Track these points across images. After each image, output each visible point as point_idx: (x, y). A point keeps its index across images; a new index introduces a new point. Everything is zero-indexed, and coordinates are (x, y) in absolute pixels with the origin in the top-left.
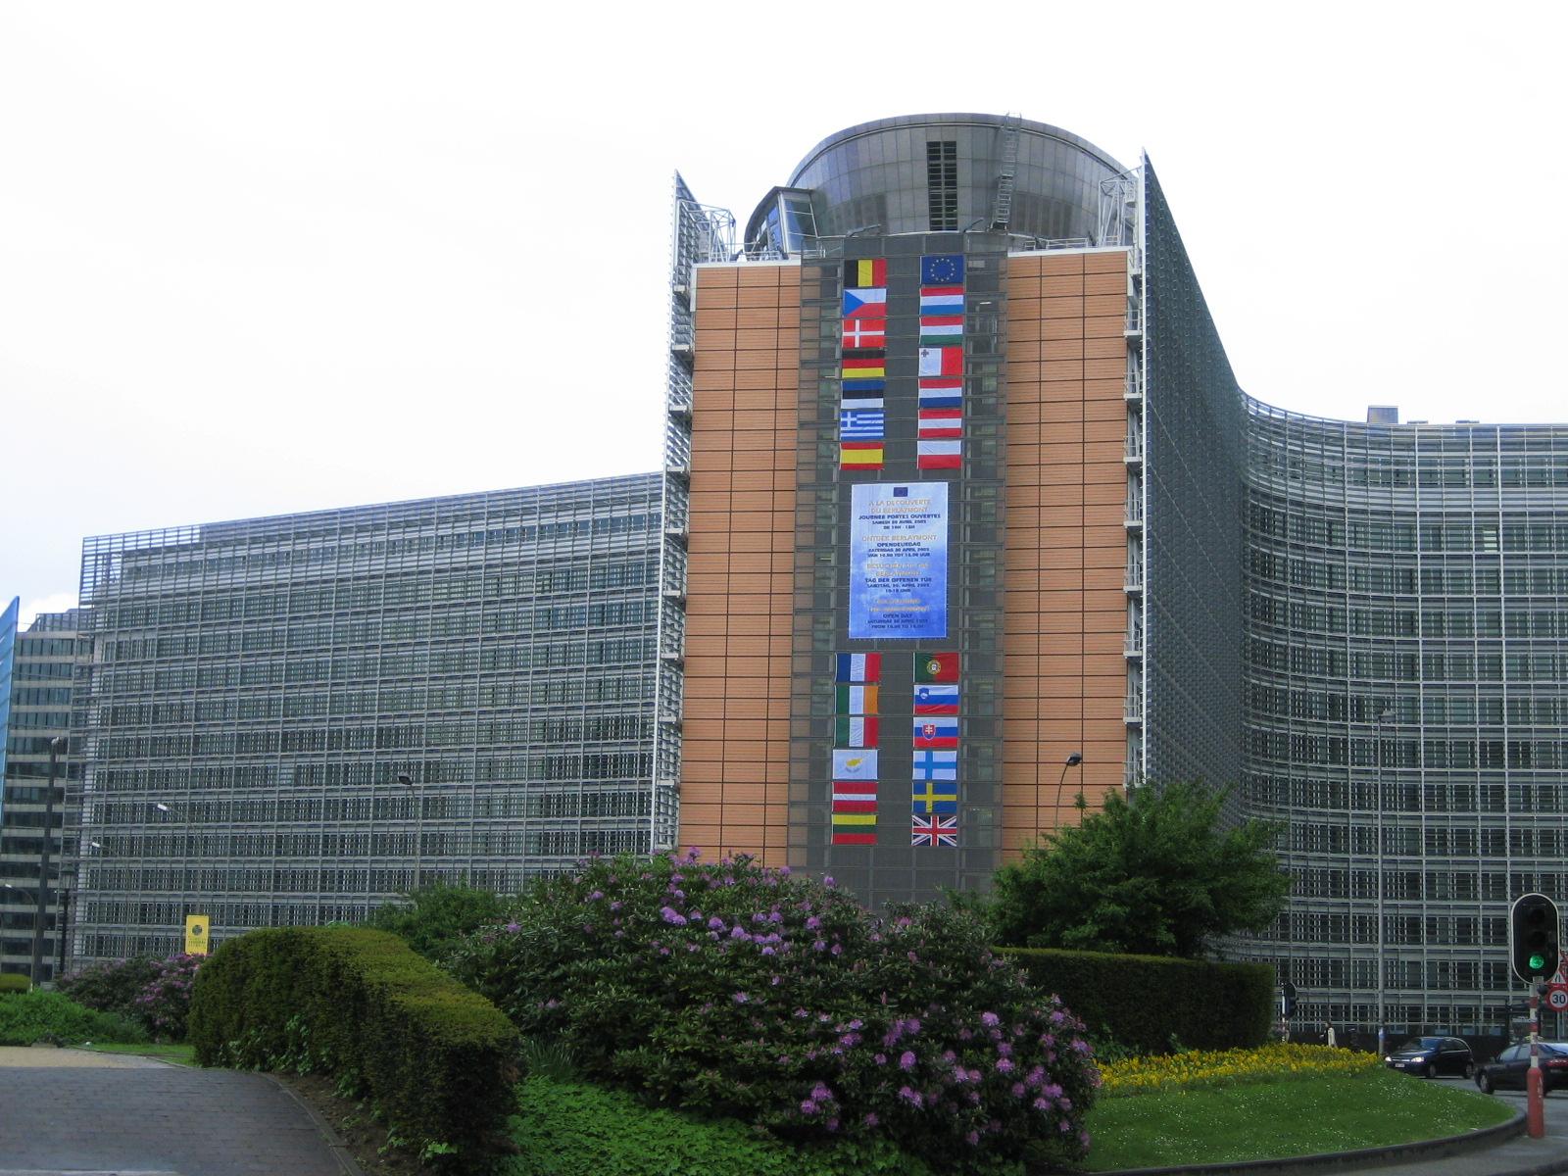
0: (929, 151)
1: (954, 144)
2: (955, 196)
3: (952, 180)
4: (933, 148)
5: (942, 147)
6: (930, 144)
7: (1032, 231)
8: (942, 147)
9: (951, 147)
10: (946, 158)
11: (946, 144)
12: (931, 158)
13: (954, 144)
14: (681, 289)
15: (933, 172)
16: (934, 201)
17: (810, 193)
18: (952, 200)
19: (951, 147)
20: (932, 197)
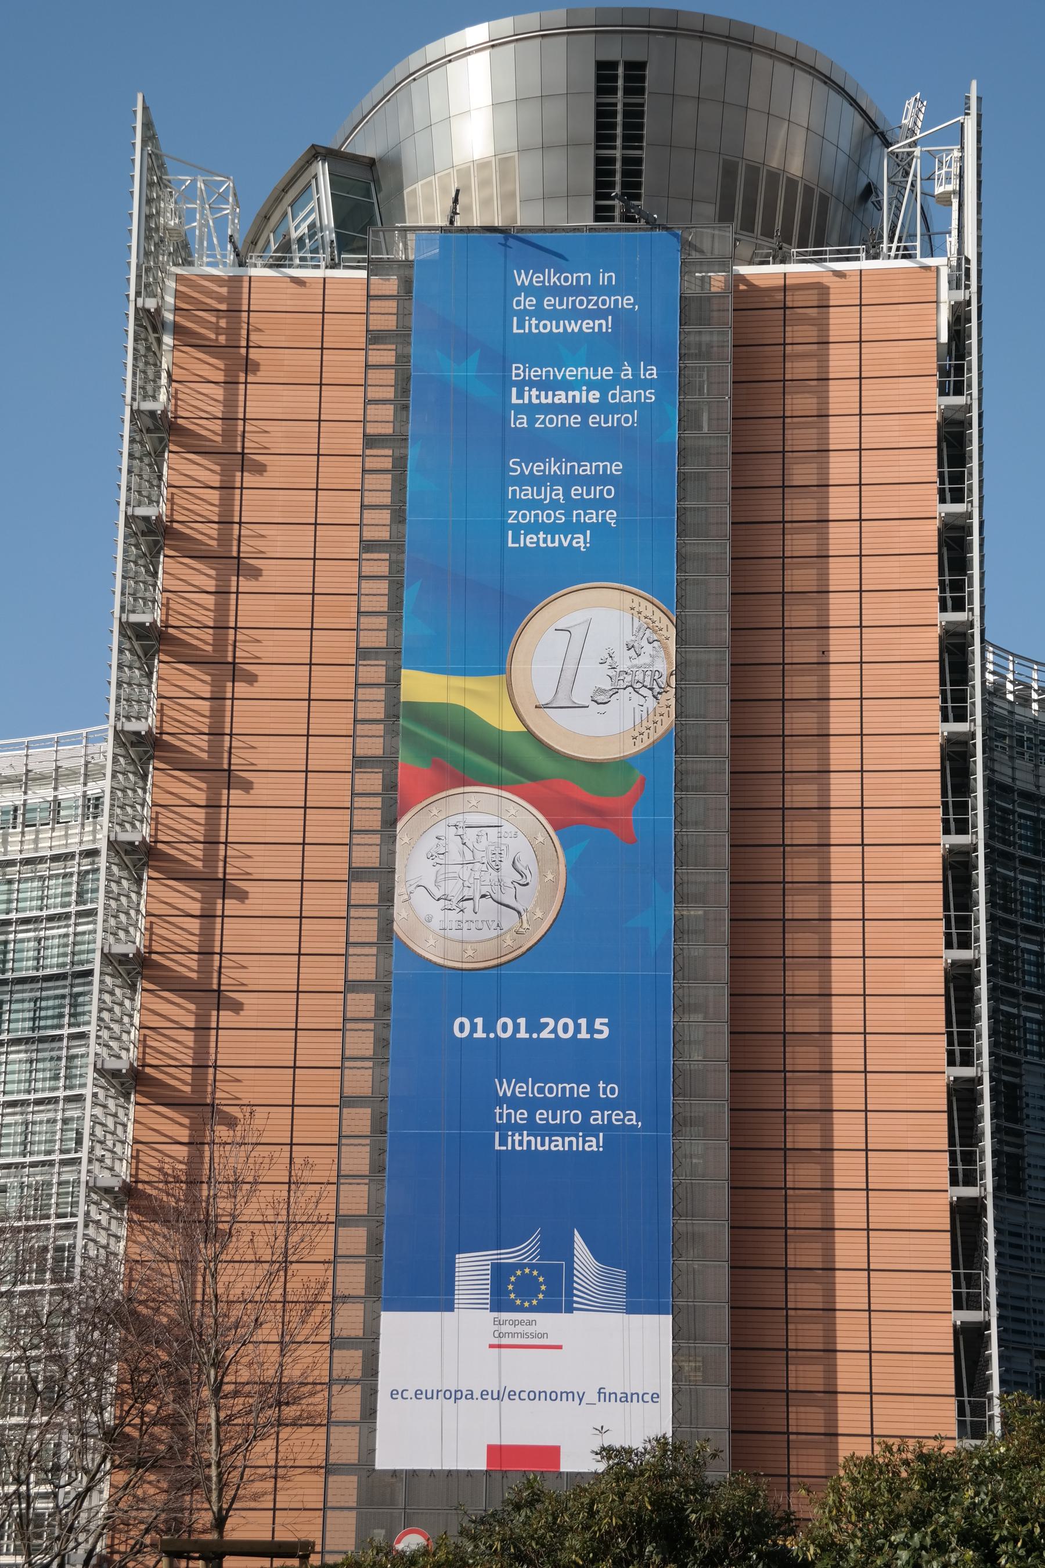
0: (599, 78)
1: (642, 66)
2: (638, 161)
4: (605, 71)
5: (621, 71)
6: (601, 65)
7: (768, 233)
8: (621, 71)
9: (636, 70)
10: (627, 91)
11: (629, 65)
12: (600, 91)
13: (642, 66)
14: (151, 304)
15: (604, 117)
17: (371, 163)
19: (636, 70)
20: (599, 161)
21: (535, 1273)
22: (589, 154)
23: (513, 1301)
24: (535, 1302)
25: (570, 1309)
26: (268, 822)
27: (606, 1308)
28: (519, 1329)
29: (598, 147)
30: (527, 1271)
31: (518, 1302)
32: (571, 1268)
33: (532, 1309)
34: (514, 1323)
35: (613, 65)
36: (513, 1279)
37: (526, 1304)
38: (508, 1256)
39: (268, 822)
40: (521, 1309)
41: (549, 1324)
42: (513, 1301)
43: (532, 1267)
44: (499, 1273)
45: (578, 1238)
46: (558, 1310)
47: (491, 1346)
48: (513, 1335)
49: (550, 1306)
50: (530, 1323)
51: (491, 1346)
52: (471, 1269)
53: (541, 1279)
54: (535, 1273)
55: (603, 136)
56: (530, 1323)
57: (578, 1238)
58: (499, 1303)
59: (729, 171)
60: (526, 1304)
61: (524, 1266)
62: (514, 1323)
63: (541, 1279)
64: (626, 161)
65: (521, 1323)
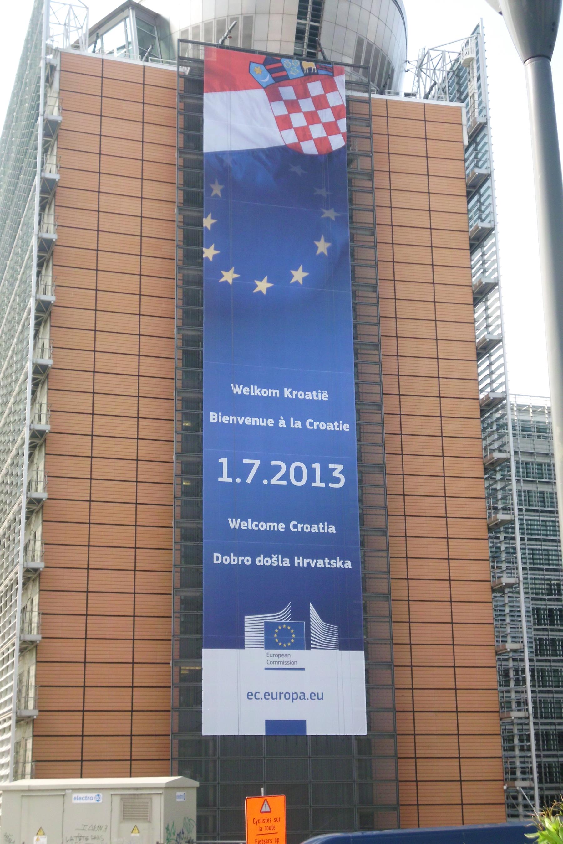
3: (317, 15)
21: (289, 628)
23: (277, 643)
24: (289, 644)
25: (309, 648)
26: (118, 362)
27: (329, 647)
28: (281, 659)
29: (299, 18)
30: (284, 626)
31: (280, 644)
32: (308, 625)
33: (288, 648)
34: (278, 656)
36: (277, 631)
37: (285, 645)
38: (272, 618)
39: (118, 362)
40: (281, 648)
41: (298, 656)
42: (277, 643)
43: (287, 624)
44: (269, 628)
45: (312, 608)
46: (301, 648)
47: (266, 669)
48: (278, 662)
49: (297, 646)
50: (287, 656)
51: (266, 669)
52: (254, 625)
53: (292, 631)
54: (289, 628)
56: (287, 656)
57: (312, 608)
58: (270, 644)
59: (360, 42)
60: (285, 645)
61: (283, 623)
62: (278, 656)
63: (292, 631)
64: (312, 27)
65: (282, 655)
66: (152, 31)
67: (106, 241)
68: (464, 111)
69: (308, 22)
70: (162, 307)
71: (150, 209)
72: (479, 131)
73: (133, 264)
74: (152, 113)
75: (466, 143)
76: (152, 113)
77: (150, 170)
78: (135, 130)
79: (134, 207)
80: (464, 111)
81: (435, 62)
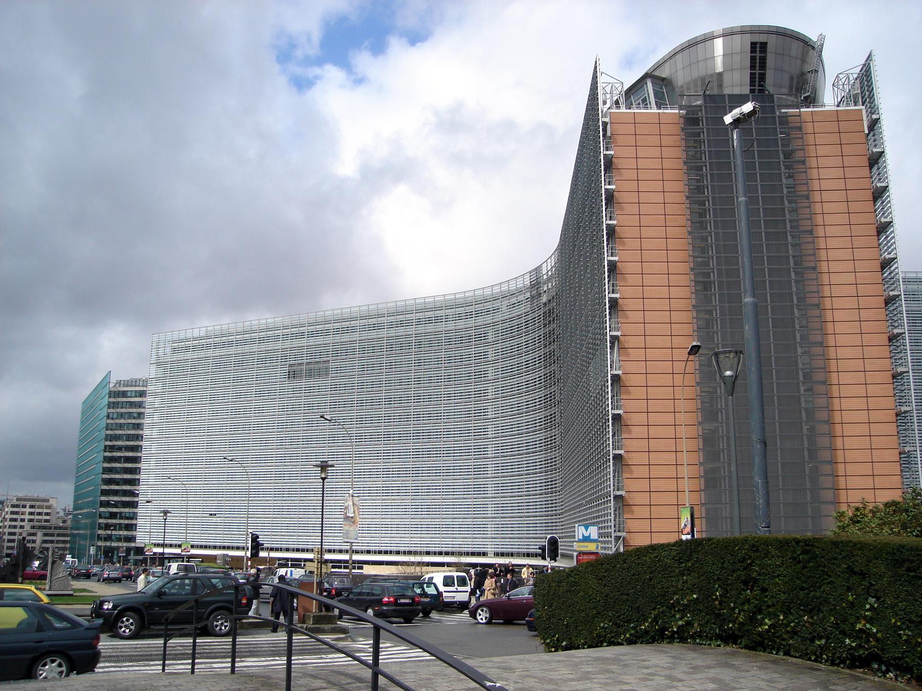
3: (763, 65)
4: (753, 45)
5: (758, 45)
6: (752, 43)
8: (758, 45)
9: (764, 45)
10: (760, 52)
12: (752, 52)
15: (753, 59)
16: (752, 76)
18: (762, 77)
19: (764, 45)
22: (748, 71)
35: (755, 43)
55: (753, 67)
66: (662, 88)
67: (645, 220)
68: (864, 112)
69: (758, 72)
70: (680, 256)
71: (669, 198)
72: (874, 124)
73: (661, 232)
74: (666, 140)
75: (867, 132)
76: (666, 140)
77: (668, 175)
78: (656, 152)
79: (659, 198)
80: (864, 112)
81: (843, 80)
